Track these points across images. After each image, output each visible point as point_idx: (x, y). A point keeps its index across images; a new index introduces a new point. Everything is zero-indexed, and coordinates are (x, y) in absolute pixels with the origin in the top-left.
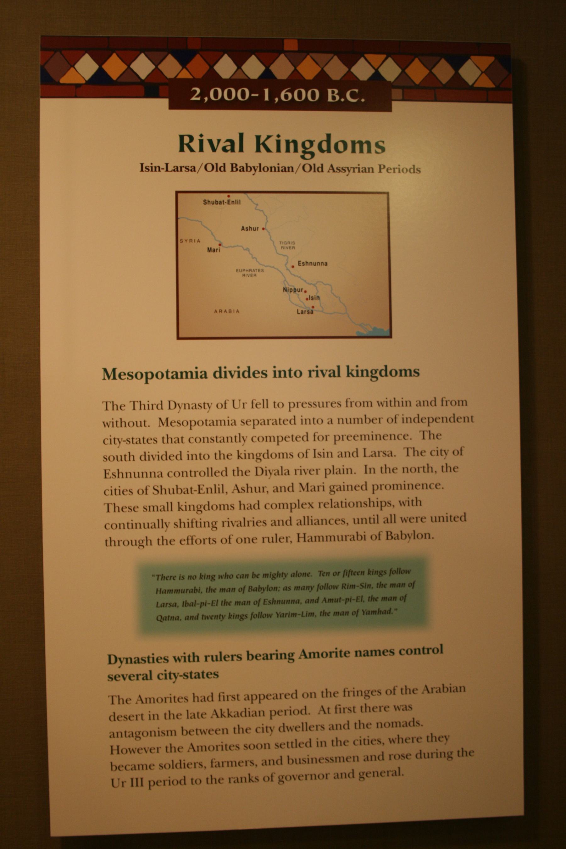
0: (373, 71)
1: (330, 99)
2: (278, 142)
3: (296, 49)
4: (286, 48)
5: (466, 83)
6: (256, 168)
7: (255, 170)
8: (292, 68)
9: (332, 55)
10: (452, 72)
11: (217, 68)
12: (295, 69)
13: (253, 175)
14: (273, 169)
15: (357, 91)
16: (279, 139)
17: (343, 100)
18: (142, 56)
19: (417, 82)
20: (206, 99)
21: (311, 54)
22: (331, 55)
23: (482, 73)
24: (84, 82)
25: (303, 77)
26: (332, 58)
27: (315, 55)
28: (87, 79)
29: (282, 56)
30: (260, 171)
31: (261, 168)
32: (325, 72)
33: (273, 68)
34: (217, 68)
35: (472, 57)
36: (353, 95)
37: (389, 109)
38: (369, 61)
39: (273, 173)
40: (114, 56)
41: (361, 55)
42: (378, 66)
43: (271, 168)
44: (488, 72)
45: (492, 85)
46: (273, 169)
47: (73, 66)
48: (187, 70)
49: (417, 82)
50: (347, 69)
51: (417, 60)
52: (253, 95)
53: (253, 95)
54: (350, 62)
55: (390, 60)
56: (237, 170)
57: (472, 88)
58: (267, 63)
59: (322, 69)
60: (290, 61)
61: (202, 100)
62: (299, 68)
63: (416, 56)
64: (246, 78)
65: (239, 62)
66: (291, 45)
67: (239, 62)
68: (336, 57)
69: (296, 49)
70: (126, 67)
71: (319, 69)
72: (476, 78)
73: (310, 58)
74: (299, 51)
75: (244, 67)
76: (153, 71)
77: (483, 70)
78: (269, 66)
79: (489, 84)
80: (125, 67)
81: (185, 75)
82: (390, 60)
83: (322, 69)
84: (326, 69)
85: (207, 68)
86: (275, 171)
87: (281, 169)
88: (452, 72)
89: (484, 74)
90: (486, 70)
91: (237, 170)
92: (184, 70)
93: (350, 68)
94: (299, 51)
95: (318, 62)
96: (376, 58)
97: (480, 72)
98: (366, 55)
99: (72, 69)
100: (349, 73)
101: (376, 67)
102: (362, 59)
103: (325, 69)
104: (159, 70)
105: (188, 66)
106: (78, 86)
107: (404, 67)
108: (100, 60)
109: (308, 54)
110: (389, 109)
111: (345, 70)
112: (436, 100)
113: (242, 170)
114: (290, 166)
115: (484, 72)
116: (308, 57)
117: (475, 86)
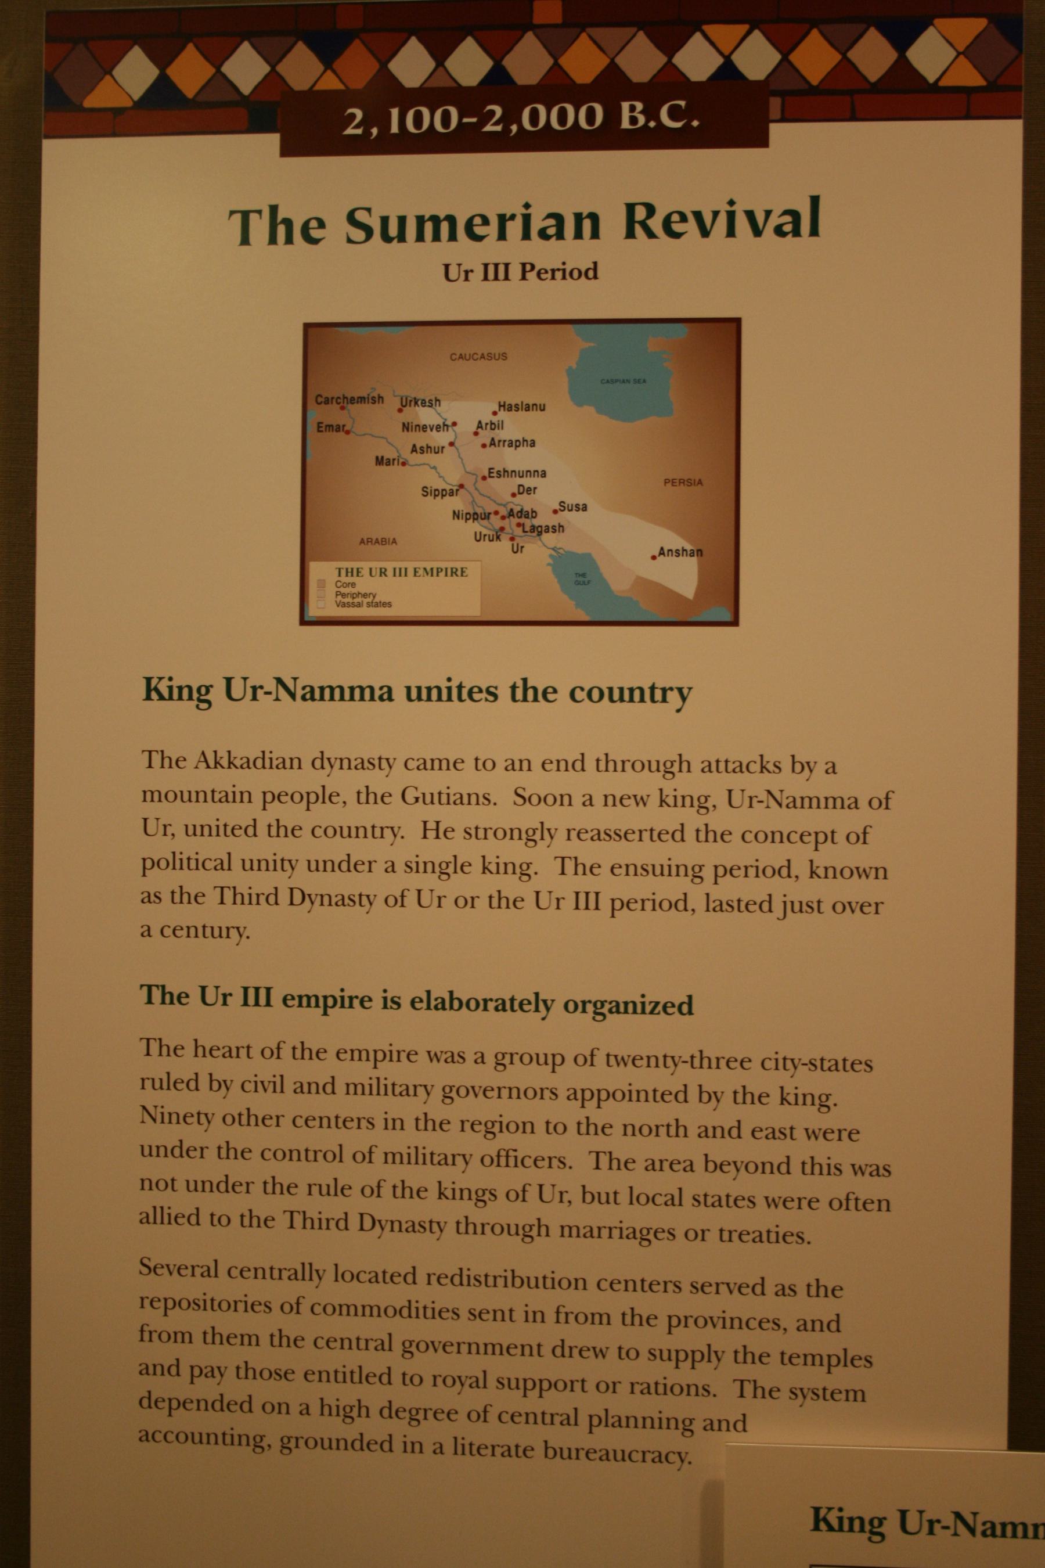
0: (720, 61)
3: (559, 20)
4: (537, 20)
8: (550, 62)
9: (635, 29)
11: (395, 66)
19: (815, 80)
21: (589, 30)
22: (632, 30)
25: (571, 79)
27: (598, 32)
29: (530, 37)
33: (509, 63)
34: (395, 66)
41: (695, 26)
48: (334, 72)
49: (815, 80)
50: (664, 59)
54: (669, 45)
55: (757, 34)
58: (497, 52)
59: (612, 61)
60: (545, 46)
62: (563, 61)
65: (440, 53)
67: (440, 53)
68: (641, 34)
69: (559, 20)
71: (606, 61)
73: (588, 38)
74: (565, 25)
75: (449, 63)
81: (330, 83)
83: (612, 61)
84: (620, 61)
85: (375, 66)
92: (329, 72)
93: (670, 54)
94: (565, 25)
95: (602, 45)
96: (725, 33)
98: (705, 28)
100: (669, 66)
101: (726, 53)
102: (698, 36)
103: (618, 60)
105: (336, 65)
107: (786, 48)
109: (583, 30)
111: (660, 59)
112: (853, 117)
116: (584, 35)
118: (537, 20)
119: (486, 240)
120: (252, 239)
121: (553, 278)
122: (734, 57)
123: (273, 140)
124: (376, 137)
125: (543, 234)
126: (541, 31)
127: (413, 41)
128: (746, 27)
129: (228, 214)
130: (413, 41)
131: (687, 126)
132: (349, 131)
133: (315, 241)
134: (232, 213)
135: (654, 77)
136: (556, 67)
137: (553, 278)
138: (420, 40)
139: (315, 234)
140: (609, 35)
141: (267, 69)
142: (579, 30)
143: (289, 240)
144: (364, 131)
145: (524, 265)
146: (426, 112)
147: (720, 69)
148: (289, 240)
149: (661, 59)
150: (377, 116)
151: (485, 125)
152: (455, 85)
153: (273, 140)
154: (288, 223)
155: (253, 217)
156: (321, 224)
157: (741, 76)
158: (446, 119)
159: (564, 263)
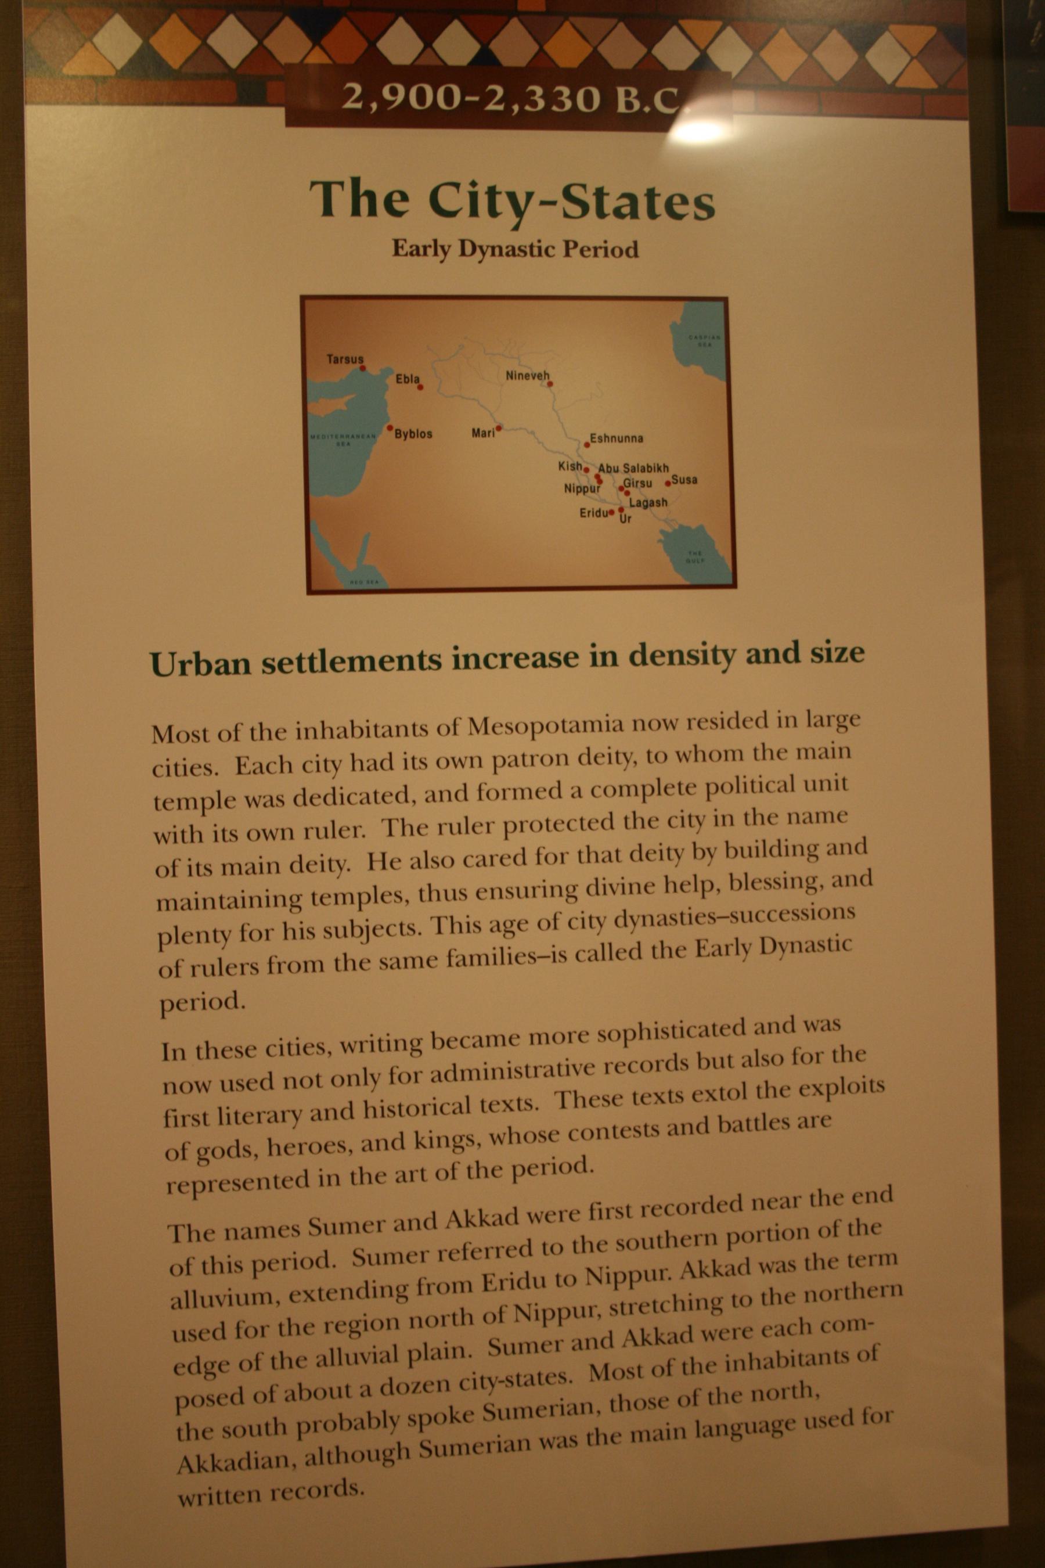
0: (697, 54)
2: (474, 196)
3: (543, 8)
4: (521, 7)
8: (535, 48)
9: (615, 21)
12: (541, 50)
16: (476, 189)
20: (374, 106)
21: (572, 19)
22: (609, 22)
23: (912, 58)
26: (616, 26)
27: (579, 21)
29: (515, 24)
33: (495, 46)
38: (688, 32)
42: (706, 44)
44: (923, 55)
45: (934, 86)
48: (323, 48)
50: (643, 50)
54: (650, 37)
58: (484, 36)
59: (595, 49)
60: (530, 33)
61: (367, 107)
62: (547, 48)
64: (440, 63)
65: (428, 35)
67: (428, 35)
68: (621, 26)
69: (543, 8)
74: (549, 12)
75: (437, 45)
77: (915, 54)
78: (489, 43)
81: (318, 57)
83: (595, 49)
84: (604, 50)
85: (364, 45)
92: (317, 49)
93: (650, 46)
94: (549, 12)
97: (908, 58)
98: (681, 22)
102: (675, 30)
105: (324, 42)
109: (566, 19)
115: (916, 58)
116: (567, 25)
117: (899, 85)
118: (521, 7)
119: (685, 219)
120: (334, 211)
121: (596, 255)
122: (710, 52)
123: (280, 113)
124: (375, 113)
125: (618, 213)
127: (401, 22)
129: (309, 184)
130: (401, 22)
132: (349, 105)
133: (399, 214)
134: (313, 184)
135: (636, 65)
136: (541, 50)
137: (596, 255)
138: (408, 21)
139: (398, 206)
141: (254, 43)
143: (372, 212)
144: (363, 105)
146: (429, 90)
148: (372, 212)
149: (643, 50)
150: (371, 93)
151: (487, 103)
152: (442, 64)
153: (280, 113)
154: (371, 195)
155: (335, 189)
156: (404, 197)
158: (449, 97)
159: (606, 242)
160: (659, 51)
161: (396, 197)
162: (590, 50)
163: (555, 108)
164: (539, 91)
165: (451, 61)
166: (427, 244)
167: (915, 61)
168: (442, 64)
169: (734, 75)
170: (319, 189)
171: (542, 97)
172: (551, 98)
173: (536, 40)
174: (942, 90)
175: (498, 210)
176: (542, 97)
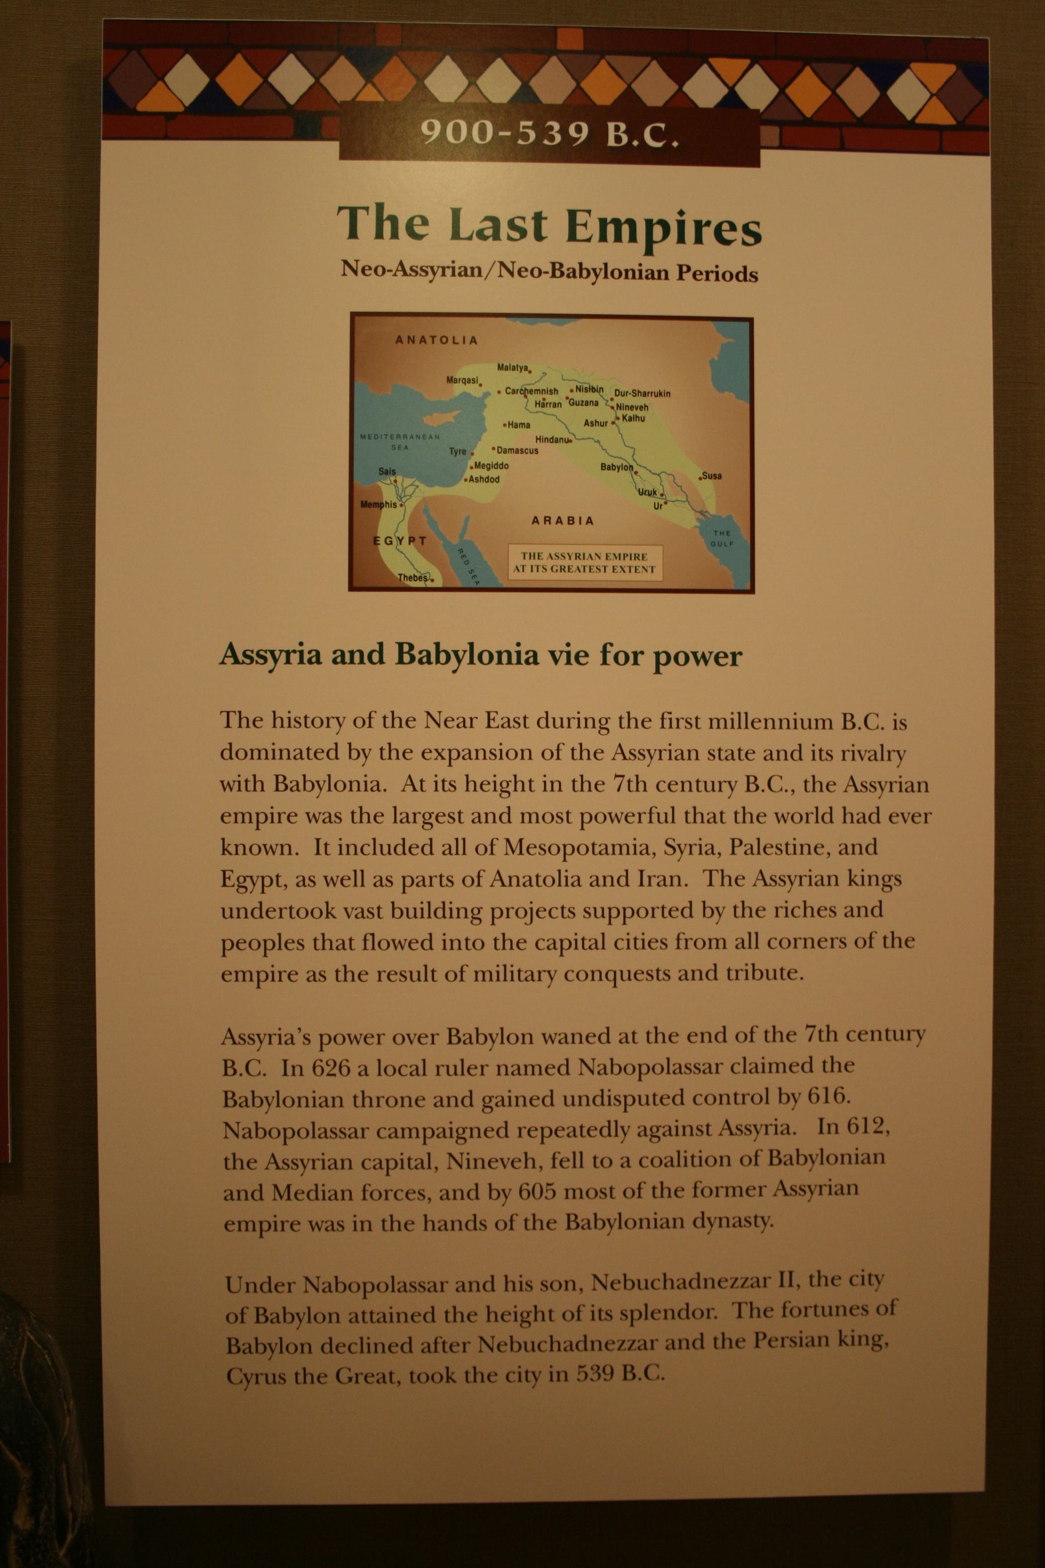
0: (725, 91)
1: (612, 142)
3: (581, 48)
4: (561, 45)
5: (903, 117)
6: (598, 271)
7: (597, 276)
9: (649, 59)
10: (874, 94)
12: (578, 87)
13: (593, 284)
14: (630, 274)
15: (662, 126)
17: (635, 143)
18: (291, 57)
19: (809, 112)
21: (607, 57)
22: (645, 60)
23: (932, 95)
24: (182, 109)
26: (649, 64)
27: (618, 60)
28: (187, 103)
29: (554, 60)
30: (606, 277)
31: (607, 272)
32: (633, 91)
33: (535, 83)
35: (913, 65)
36: (656, 135)
37: (755, 163)
39: (630, 281)
40: (239, 59)
41: (703, 59)
43: (627, 271)
44: (943, 94)
45: (950, 121)
46: (630, 274)
47: (162, 78)
48: (374, 85)
49: (809, 112)
50: (674, 87)
51: (808, 70)
52: (501, 134)
53: (501, 134)
54: (681, 74)
55: (757, 69)
56: (562, 274)
57: (912, 125)
59: (629, 86)
62: (583, 85)
63: (807, 62)
64: (484, 101)
66: (570, 39)
68: (654, 63)
69: (581, 48)
70: (259, 80)
72: (920, 107)
74: (586, 51)
76: (311, 88)
77: (934, 91)
79: (944, 118)
80: (259, 80)
81: (370, 95)
82: (757, 69)
83: (629, 86)
86: (634, 277)
87: (644, 274)
88: (874, 94)
89: (935, 98)
90: (940, 90)
91: (562, 274)
92: (370, 86)
93: (681, 83)
94: (586, 51)
96: (731, 66)
97: (929, 95)
98: (712, 61)
99: (160, 83)
101: (731, 84)
102: (705, 67)
103: (634, 86)
104: (321, 85)
105: (376, 80)
106: (170, 116)
107: (783, 82)
108: (212, 66)
109: (602, 57)
110: (755, 163)
111: (672, 87)
112: (842, 147)
113: (571, 275)
114: (629, 268)
116: (603, 62)
117: (918, 121)
126: (566, 56)
127: (448, 61)
128: (747, 62)
130: (448, 61)
131: (668, 146)
133: (419, 237)
134: (341, 209)
135: (667, 103)
136: (578, 87)
138: (453, 59)
139: (419, 230)
140: (627, 63)
142: (598, 57)
143: (395, 235)
145: (681, 267)
147: (726, 98)
148: (395, 235)
149: (674, 87)
152: (486, 102)
154: (393, 219)
155: (361, 213)
156: (425, 222)
157: (742, 105)
160: (689, 88)
161: (418, 221)
162: (625, 86)
163: (546, 142)
164: (556, 126)
165: (495, 100)
166: (446, 265)
167: (935, 98)
168: (486, 102)
169: (761, 111)
170: (346, 213)
171: (559, 132)
172: (543, 132)
173: (573, 77)
174: (961, 126)
175: (544, 234)
176: (559, 132)
